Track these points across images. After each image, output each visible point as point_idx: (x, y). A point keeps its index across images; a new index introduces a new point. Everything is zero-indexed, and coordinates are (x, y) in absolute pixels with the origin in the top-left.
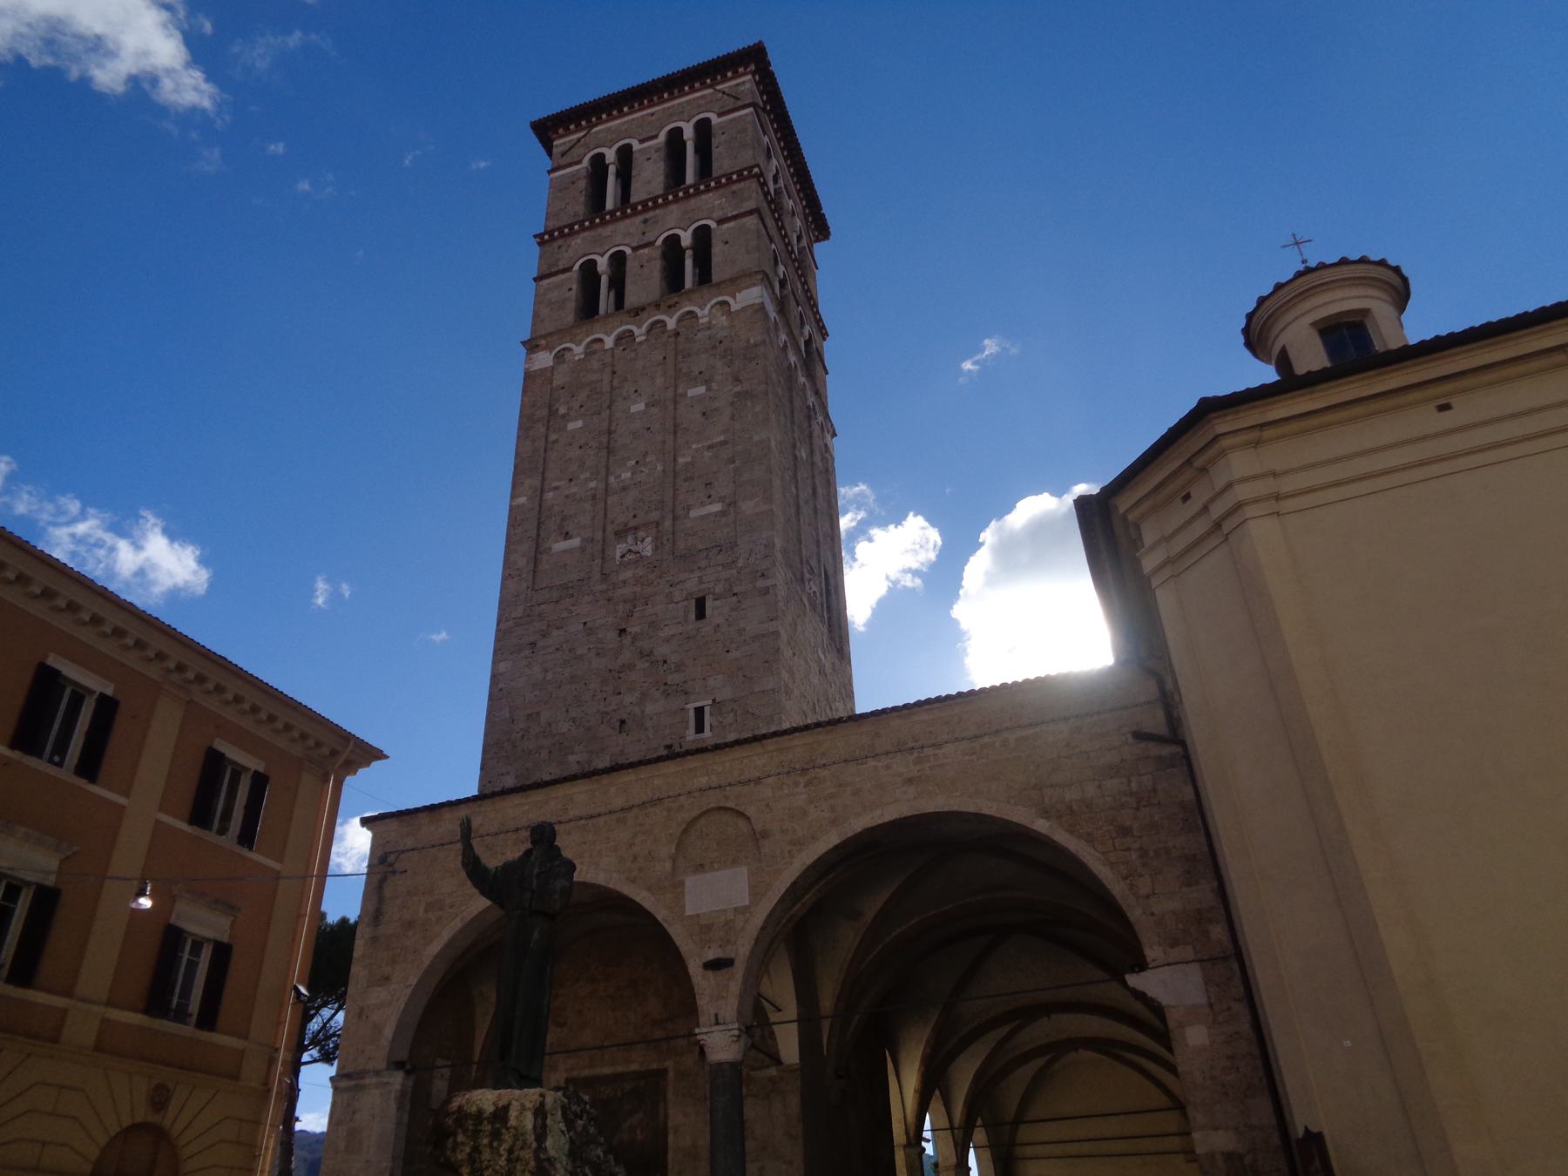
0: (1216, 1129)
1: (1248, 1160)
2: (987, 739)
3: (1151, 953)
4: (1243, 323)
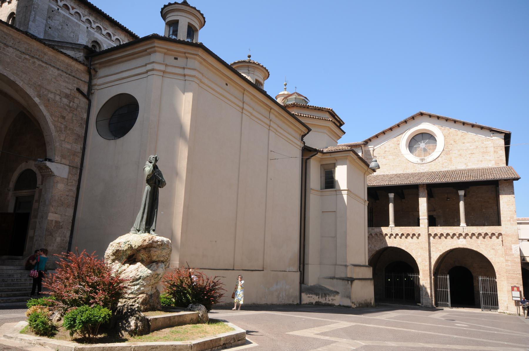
1: (61, 224)
2: (27, 57)
3: (57, 158)
4: (172, 2)
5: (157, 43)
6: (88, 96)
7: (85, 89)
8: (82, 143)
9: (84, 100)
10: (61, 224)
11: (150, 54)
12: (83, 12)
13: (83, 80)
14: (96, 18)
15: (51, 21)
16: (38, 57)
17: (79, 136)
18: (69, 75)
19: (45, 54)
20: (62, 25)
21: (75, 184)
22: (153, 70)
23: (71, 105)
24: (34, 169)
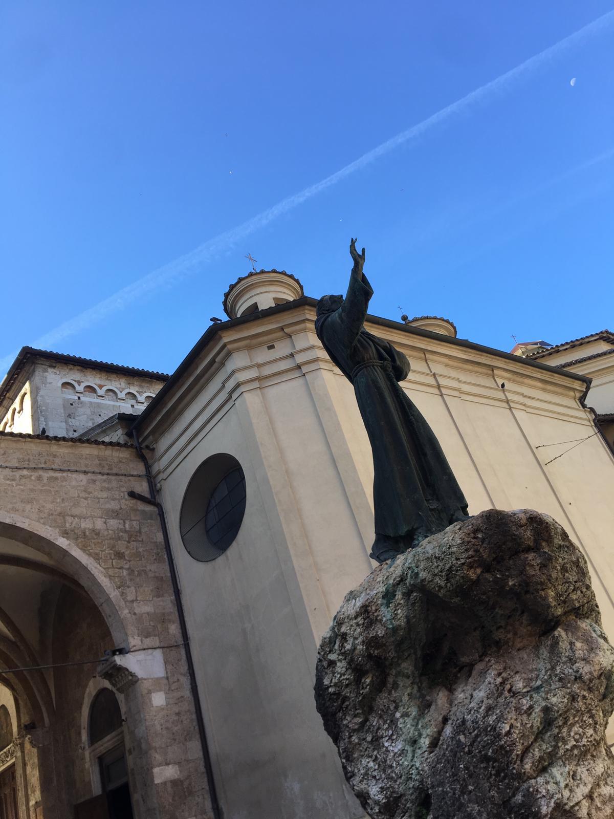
0: (167, 764)
1: (186, 784)
2: (25, 472)
3: (134, 641)
5: (227, 337)
6: (153, 499)
7: (142, 488)
8: (171, 590)
9: (149, 508)
10: (186, 784)
11: (223, 364)
12: (119, 386)
13: (135, 473)
14: (141, 386)
15: (73, 421)
16: (43, 466)
17: (160, 579)
18: (108, 474)
19: (55, 456)
20: (93, 419)
21: (185, 681)
22: (238, 386)
23: (127, 526)
24: (107, 684)
